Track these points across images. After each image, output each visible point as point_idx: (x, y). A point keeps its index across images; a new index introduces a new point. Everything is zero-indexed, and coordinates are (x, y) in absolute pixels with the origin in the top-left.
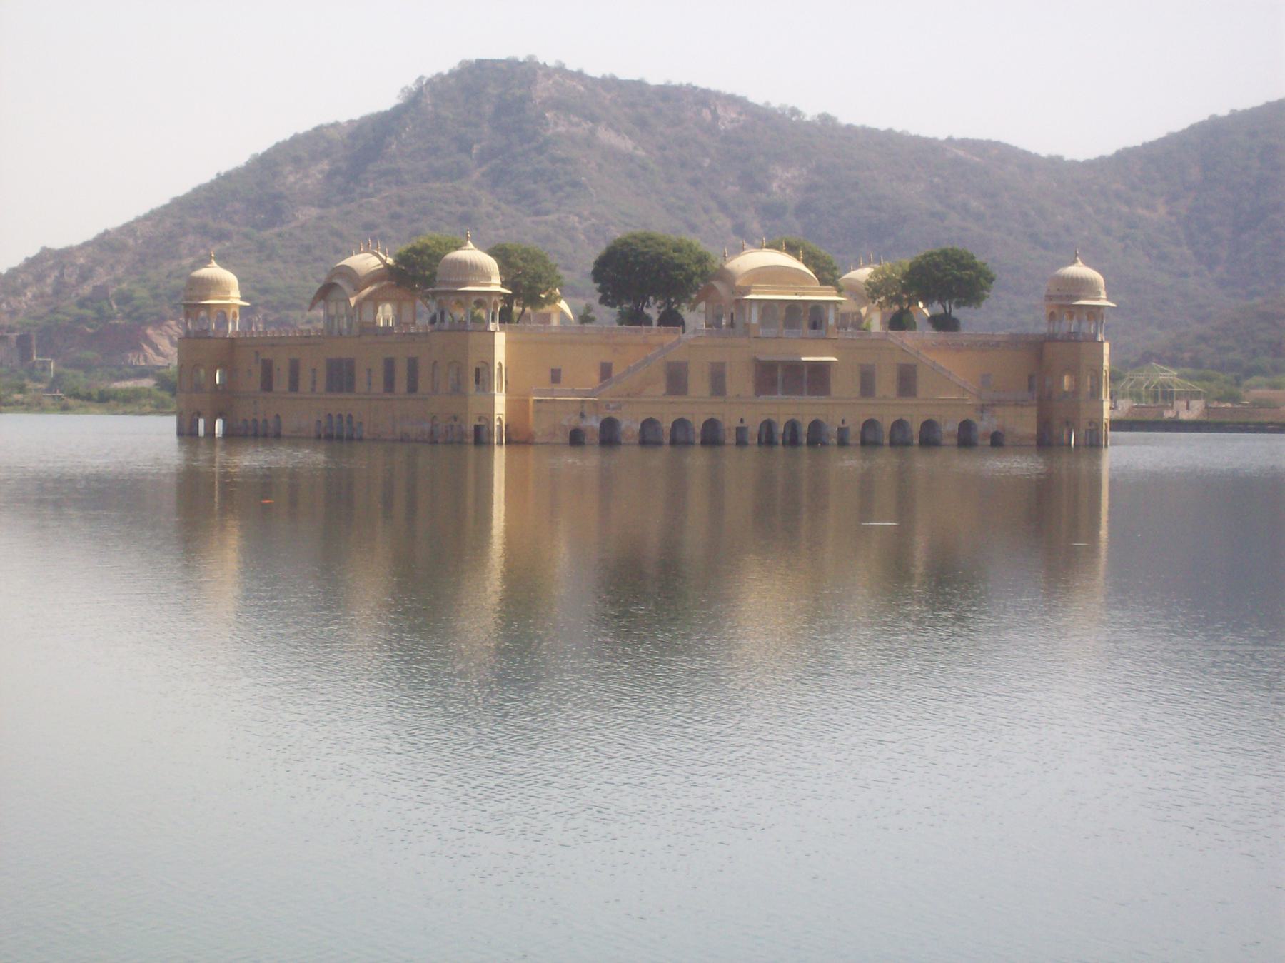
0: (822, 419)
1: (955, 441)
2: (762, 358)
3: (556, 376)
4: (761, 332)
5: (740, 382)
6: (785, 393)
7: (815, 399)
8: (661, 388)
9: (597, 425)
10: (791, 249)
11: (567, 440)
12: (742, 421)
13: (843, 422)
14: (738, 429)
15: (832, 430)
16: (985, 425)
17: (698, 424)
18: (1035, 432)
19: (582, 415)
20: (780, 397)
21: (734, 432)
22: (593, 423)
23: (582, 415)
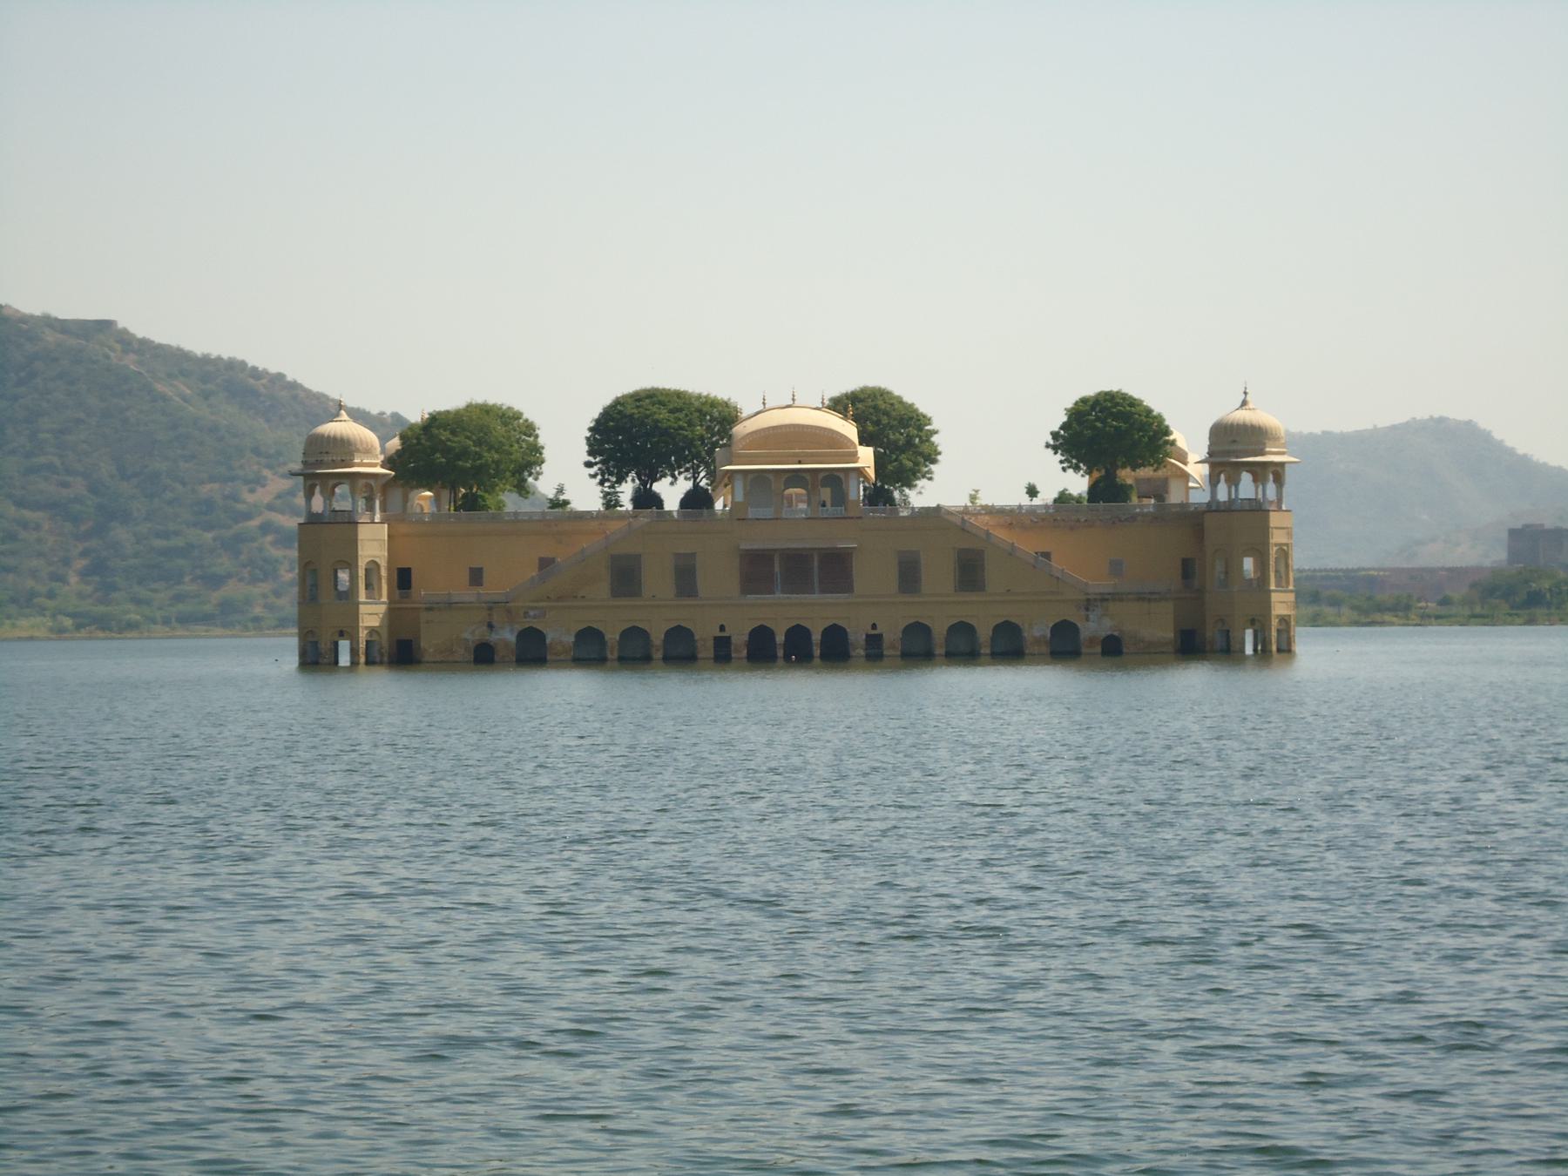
0: (840, 623)
1: (1045, 649)
2: (743, 547)
3: (476, 576)
4: (752, 513)
5: (719, 577)
6: (823, 591)
7: (830, 598)
8: (603, 589)
9: (570, 639)
10: (838, 405)
11: (472, 657)
12: (722, 628)
13: (874, 626)
14: (716, 638)
15: (857, 636)
16: (1093, 627)
17: (939, 629)
18: (1170, 635)
19: (491, 626)
20: (779, 596)
21: (711, 643)
22: (507, 636)
23: (491, 626)
